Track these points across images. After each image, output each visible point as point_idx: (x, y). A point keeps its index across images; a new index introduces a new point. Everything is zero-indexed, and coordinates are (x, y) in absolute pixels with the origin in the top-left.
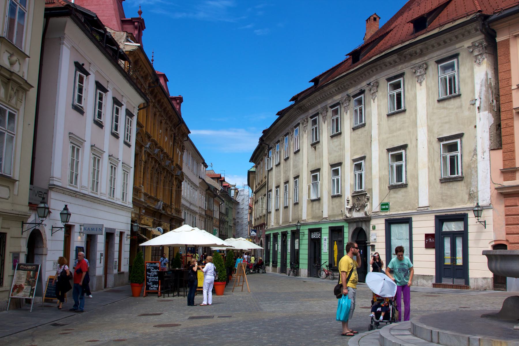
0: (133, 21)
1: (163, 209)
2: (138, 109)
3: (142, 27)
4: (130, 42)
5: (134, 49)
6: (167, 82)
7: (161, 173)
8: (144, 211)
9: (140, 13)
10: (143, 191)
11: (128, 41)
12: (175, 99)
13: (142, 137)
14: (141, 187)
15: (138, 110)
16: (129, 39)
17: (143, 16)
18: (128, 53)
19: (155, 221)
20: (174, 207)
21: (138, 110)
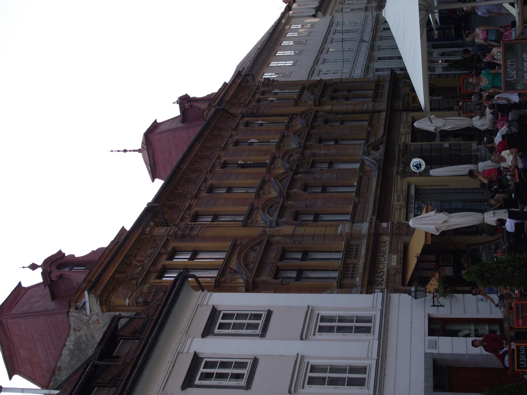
0: (49, 283)
1: (376, 148)
2: (200, 291)
3: (58, 259)
4: (85, 303)
5: (95, 300)
6: (158, 121)
7: (314, 156)
8: (385, 225)
9: (33, 267)
10: (347, 229)
11: (84, 306)
12: (183, 110)
13: (252, 248)
14: (341, 234)
15: (203, 291)
16: (80, 304)
17: (40, 262)
18: (104, 307)
19: (400, 171)
20: (369, 105)
21: (203, 291)
